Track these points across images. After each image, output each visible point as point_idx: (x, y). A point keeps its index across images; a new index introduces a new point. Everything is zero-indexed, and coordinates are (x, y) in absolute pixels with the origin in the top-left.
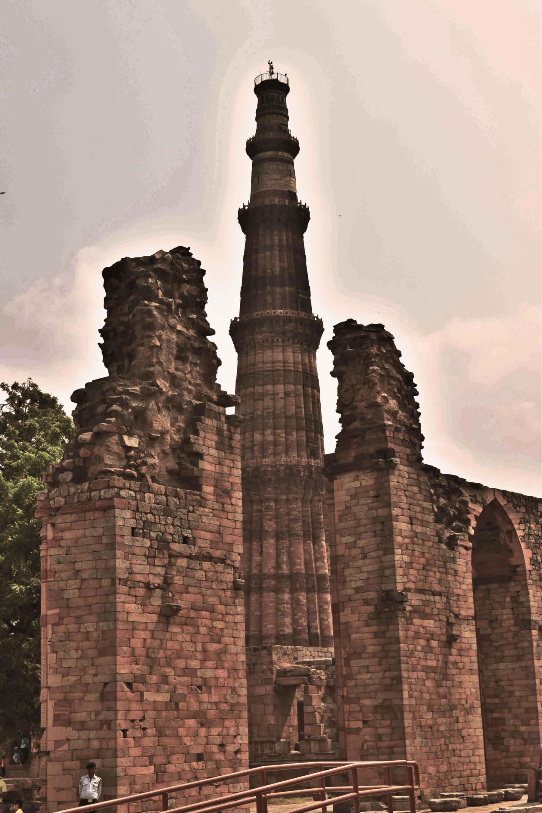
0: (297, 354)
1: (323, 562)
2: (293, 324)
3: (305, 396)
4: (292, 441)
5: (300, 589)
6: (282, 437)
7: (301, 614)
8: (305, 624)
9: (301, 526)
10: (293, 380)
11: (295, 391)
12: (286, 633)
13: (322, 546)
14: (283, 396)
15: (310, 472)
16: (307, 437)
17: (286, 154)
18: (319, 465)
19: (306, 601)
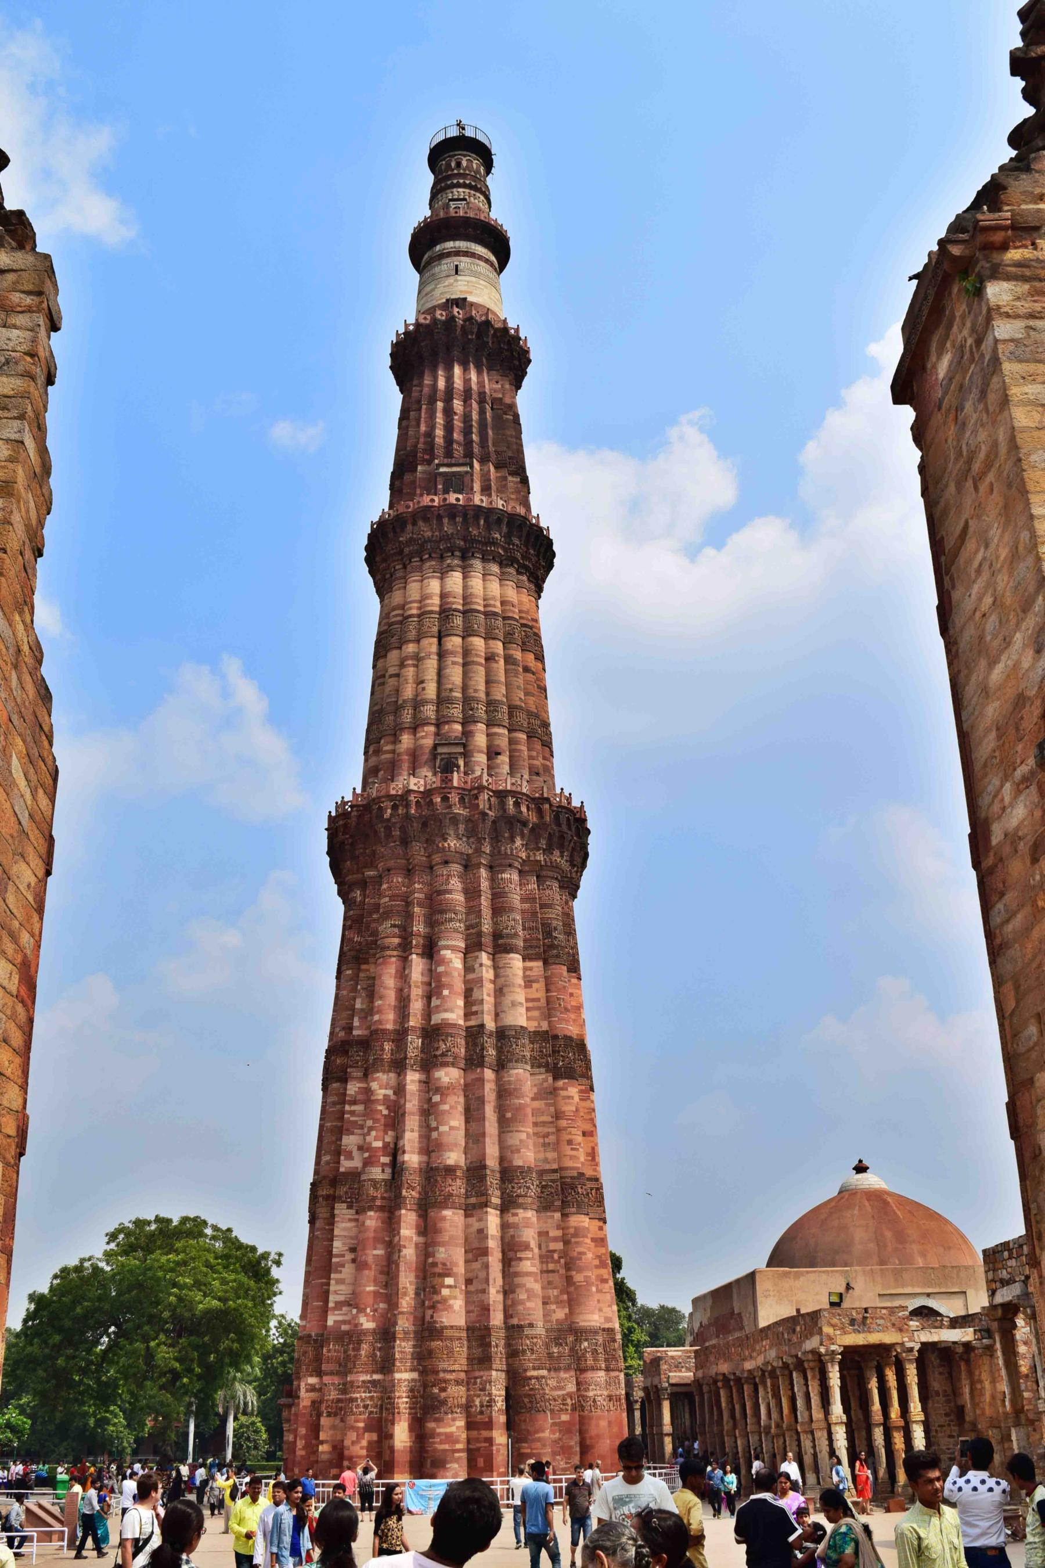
0: (426, 581)
1: (439, 995)
2: (409, 527)
3: (442, 655)
4: (399, 755)
5: (373, 1064)
6: (387, 752)
7: (370, 1123)
8: (379, 1144)
9: (394, 926)
10: (413, 634)
11: (418, 653)
12: (342, 1170)
13: (442, 961)
14: (397, 672)
15: (407, 806)
16: (437, 734)
17: (450, 245)
18: (434, 786)
19: (390, 1092)
